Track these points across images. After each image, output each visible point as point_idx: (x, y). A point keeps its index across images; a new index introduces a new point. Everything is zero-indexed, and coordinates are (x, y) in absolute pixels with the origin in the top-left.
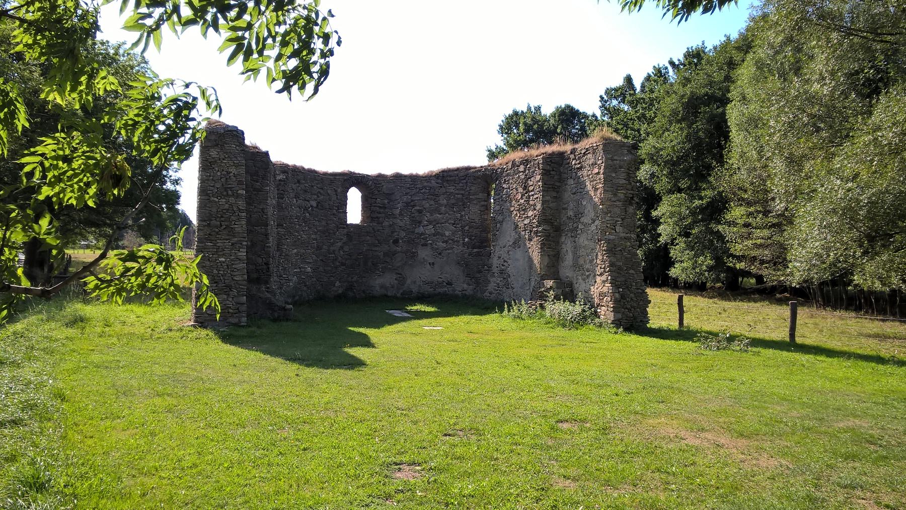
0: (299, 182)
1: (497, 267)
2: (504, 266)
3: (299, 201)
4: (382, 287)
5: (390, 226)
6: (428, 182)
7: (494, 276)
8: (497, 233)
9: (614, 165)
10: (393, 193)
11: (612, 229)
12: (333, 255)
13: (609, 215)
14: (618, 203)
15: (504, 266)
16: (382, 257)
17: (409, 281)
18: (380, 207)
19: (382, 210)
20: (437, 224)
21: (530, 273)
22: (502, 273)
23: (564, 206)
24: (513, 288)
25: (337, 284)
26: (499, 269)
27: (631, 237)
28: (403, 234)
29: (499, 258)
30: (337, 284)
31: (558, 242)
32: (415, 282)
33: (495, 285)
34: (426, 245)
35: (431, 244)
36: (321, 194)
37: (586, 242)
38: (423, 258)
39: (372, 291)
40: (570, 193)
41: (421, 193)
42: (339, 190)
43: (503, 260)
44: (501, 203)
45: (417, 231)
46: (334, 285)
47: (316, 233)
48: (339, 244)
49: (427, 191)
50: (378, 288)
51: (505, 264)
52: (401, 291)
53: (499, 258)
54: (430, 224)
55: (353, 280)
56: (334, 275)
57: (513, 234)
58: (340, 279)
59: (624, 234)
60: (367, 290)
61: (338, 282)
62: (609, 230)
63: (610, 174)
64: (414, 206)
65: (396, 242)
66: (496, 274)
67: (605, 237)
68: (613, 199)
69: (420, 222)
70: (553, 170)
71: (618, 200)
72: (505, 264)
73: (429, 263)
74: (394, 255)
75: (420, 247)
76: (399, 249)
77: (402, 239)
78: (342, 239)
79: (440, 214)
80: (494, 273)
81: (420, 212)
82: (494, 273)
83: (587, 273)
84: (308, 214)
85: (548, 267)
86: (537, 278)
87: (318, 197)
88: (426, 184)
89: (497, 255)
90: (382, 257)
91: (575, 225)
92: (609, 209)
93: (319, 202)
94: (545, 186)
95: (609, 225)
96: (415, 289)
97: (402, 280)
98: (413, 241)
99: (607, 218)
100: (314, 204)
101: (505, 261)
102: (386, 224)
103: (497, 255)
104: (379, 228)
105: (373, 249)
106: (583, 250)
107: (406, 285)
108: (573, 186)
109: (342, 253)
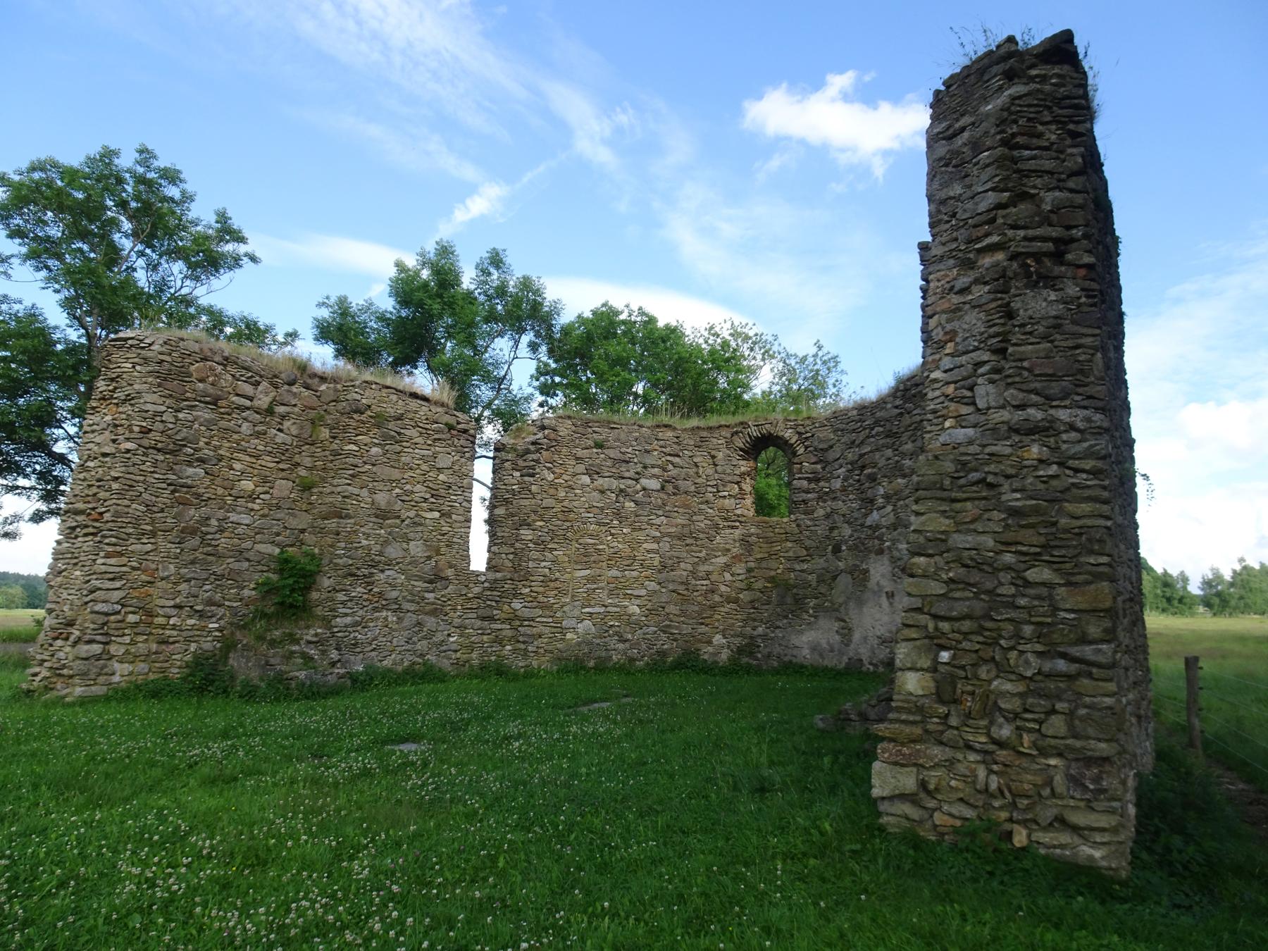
0: (599, 445)
3: (601, 481)
4: (815, 648)
5: (828, 516)
6: (883, 408)
9: (958, 153)
10: (831, 447)
11: (960, 400)
12: (704, 582)
13: (950, 348)
14: (979, 292)
16: (814, 584)
17: (857, 636)
18: (809, 480)
19: (813, 485)
20: (899, 500)
25: (718, 639)
27: (1054, 420)
28: (847, 531)
30: (718, 639)
32: (865, 638)
34: (880, 552)
35: (889, 548)
36: (672, 464)
38: (878, 584)
39: (795, 657)
41: (872, 436)
42: (720, 455)
45: (869, 521)
46: (709, 642)
47: (656, 540)
48: (722, 560)
49: (881, 429)
50: (806, 652)
52: (845, 659)
54: (888, 503)
55: (755, 633)
56: (708, 621)
58: (724, 630)
59: (1005, 415)
60: (786, 655)
61: (718, 637)
62: (953, 406)
64: (863, 467)
65: (837, 550)
67: (942, 439)
68: (963, 281)
69: (872, 501)
71: (977, 281)
73: (887, 593)
74: (834, 578)
75: (873, 555)
76: (841, 565)
77: (846, 542)
78: (728, 550)
79: (904, 476)
81: (872, 478)
84: (630, 505)
87: (665, 470)
88: (878, 414)
90: (814, 584)
93: (667, 481)
96: (865, 654)
97: (846, 633)
98: (863, 544)
99: (947, 363)
100: (654, 484)
102: (820, 512)
104: (809, 523)
105: (797, 567)
107: (852, 646)
109: (728, 576)
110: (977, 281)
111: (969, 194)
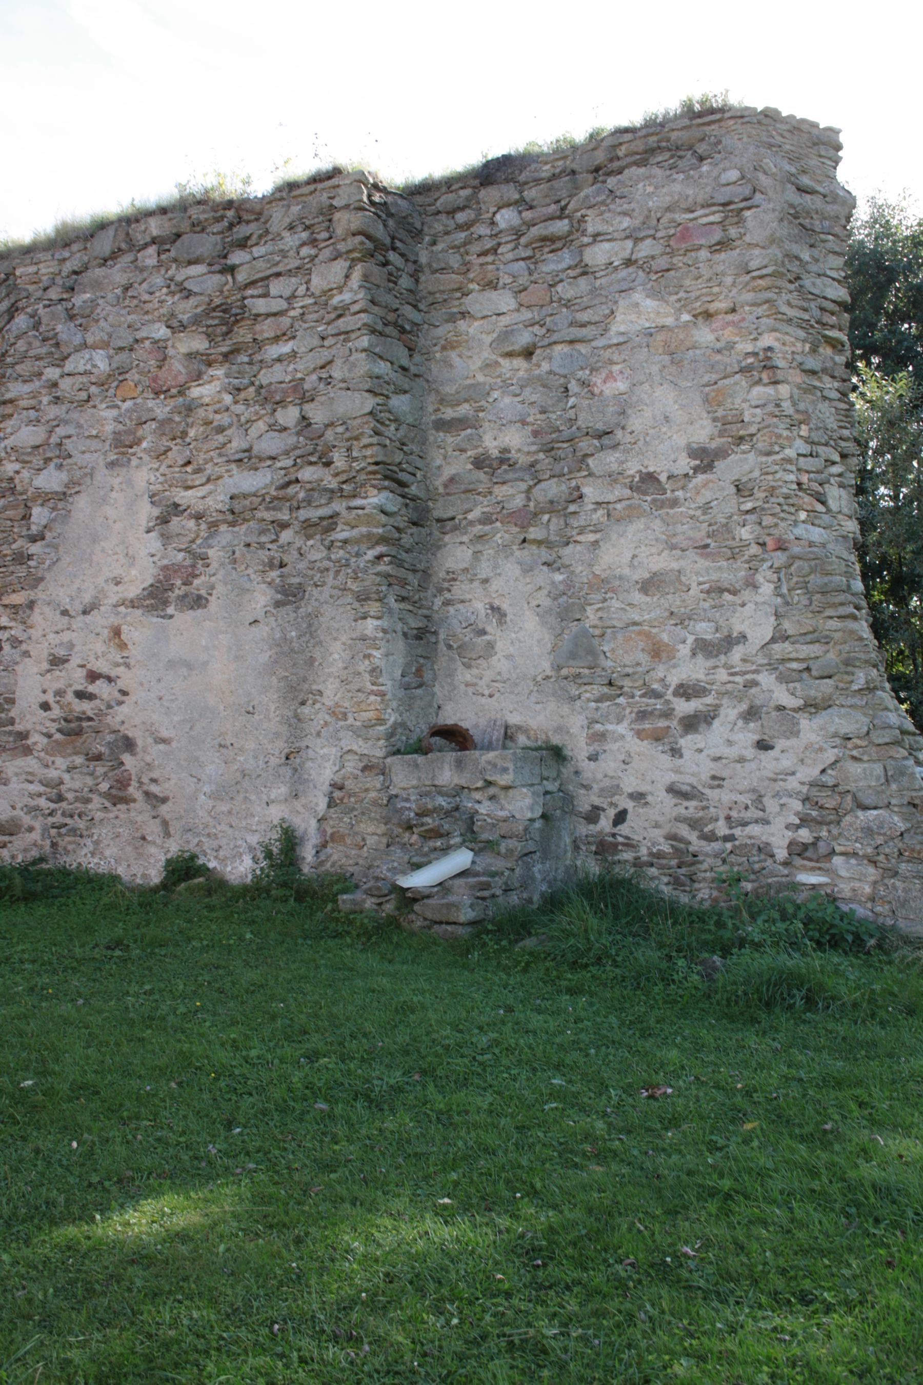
1: (45, 706)
2: (91, 697)
7: (28, 751)
8: (35, 549)
13: (804, 430)
15: (91, 697)
21: (296, 723)
22: (79, 732)
23: (449, 413)
24: (155, 800)
26: (56, 712)
29: (57, 662)
31: (426, 574)
33: (36, 788)
37: (663, 562)
40: (487, 354)
43: (81, 673)
44: (54, 411)
51: (100, 688)
53: (57, 662)
57: (153, 542)
63: (795, 249)
66: (36, 739)
70: (394, 249)
72: (100, 688)
80: (23, 736)
82: (23, 736)
83: (684, 707)
85: (407, 687)
86: (359, 746)
89: (41, 650)
91: (552, 489)
92: (802, 406)
94: (376, 309)
95: (805, 478)
101: (93, 676)
103: (41, 650)
106: (637, 597)
108: (504, 321)
110: (824, 370)
111: (814, 268)
